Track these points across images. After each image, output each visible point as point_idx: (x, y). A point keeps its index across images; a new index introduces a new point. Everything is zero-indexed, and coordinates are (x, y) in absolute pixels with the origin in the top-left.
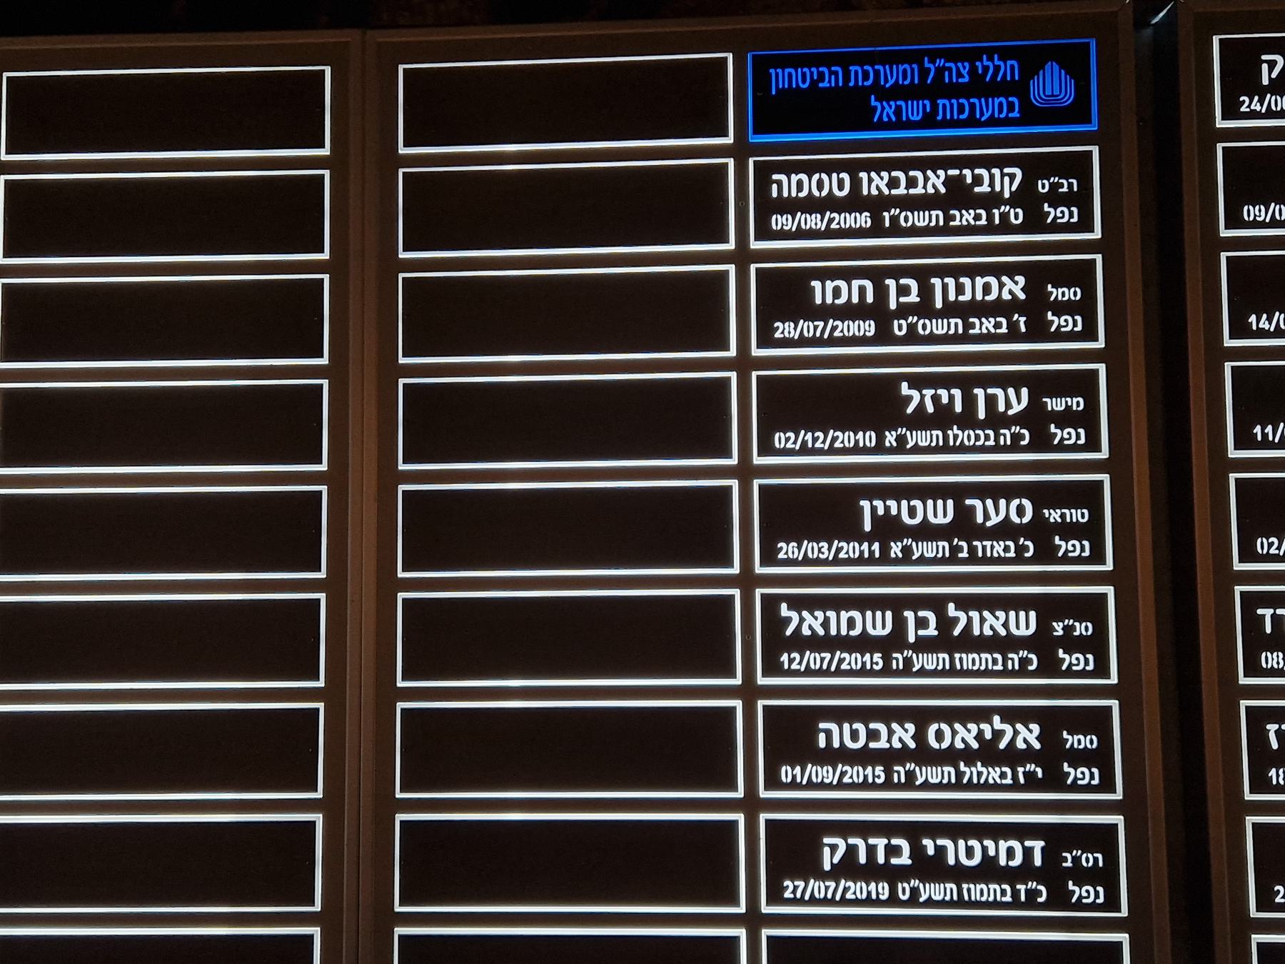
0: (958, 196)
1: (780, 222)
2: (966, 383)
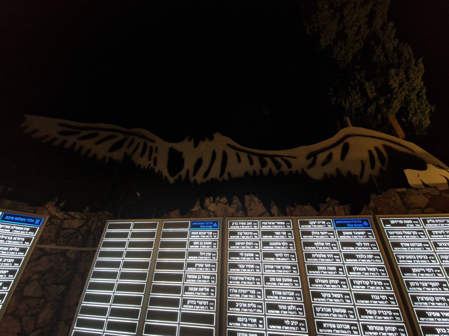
0: (207, 234)
1: (192, 236)
2: (206, 252)
